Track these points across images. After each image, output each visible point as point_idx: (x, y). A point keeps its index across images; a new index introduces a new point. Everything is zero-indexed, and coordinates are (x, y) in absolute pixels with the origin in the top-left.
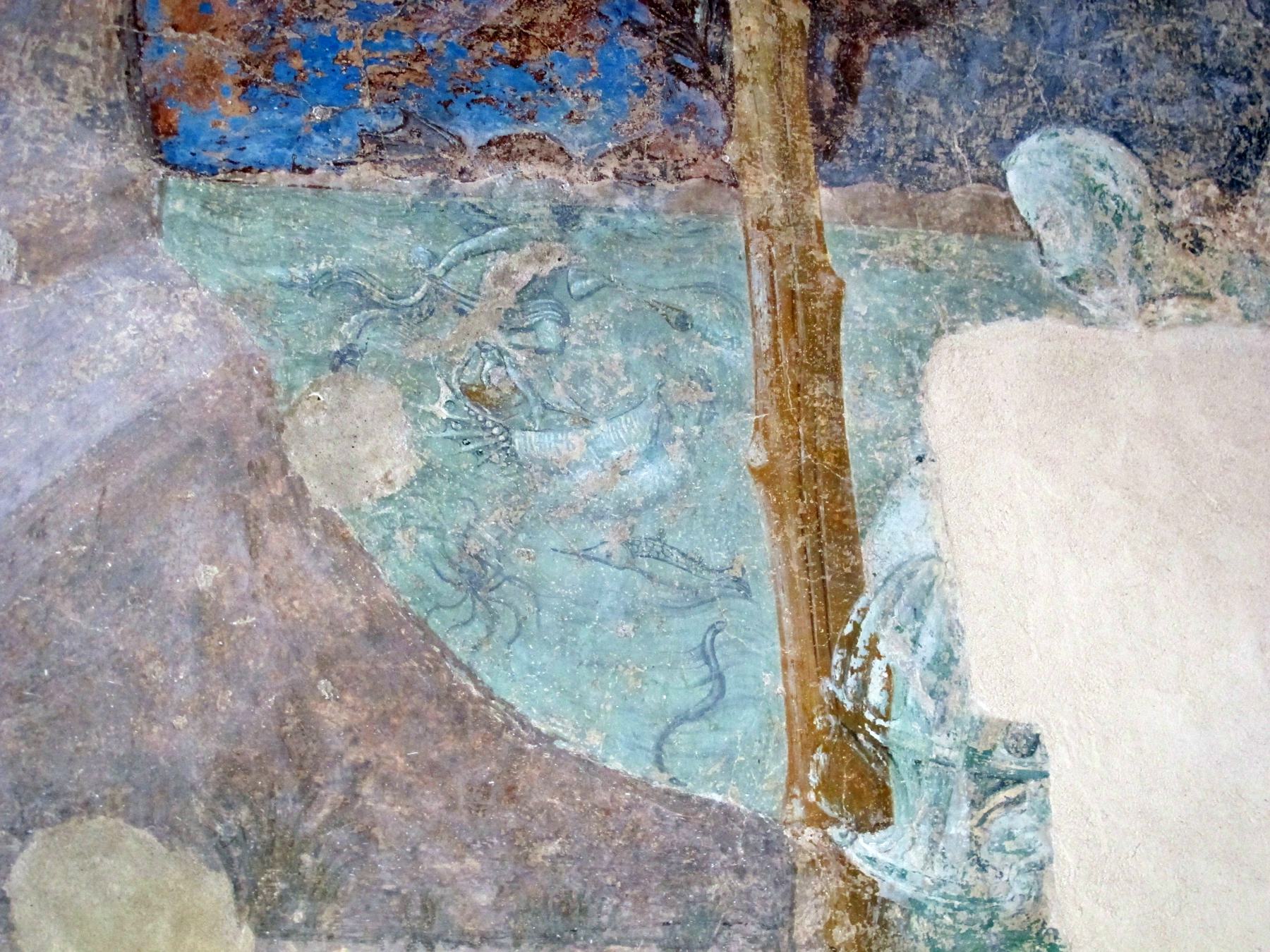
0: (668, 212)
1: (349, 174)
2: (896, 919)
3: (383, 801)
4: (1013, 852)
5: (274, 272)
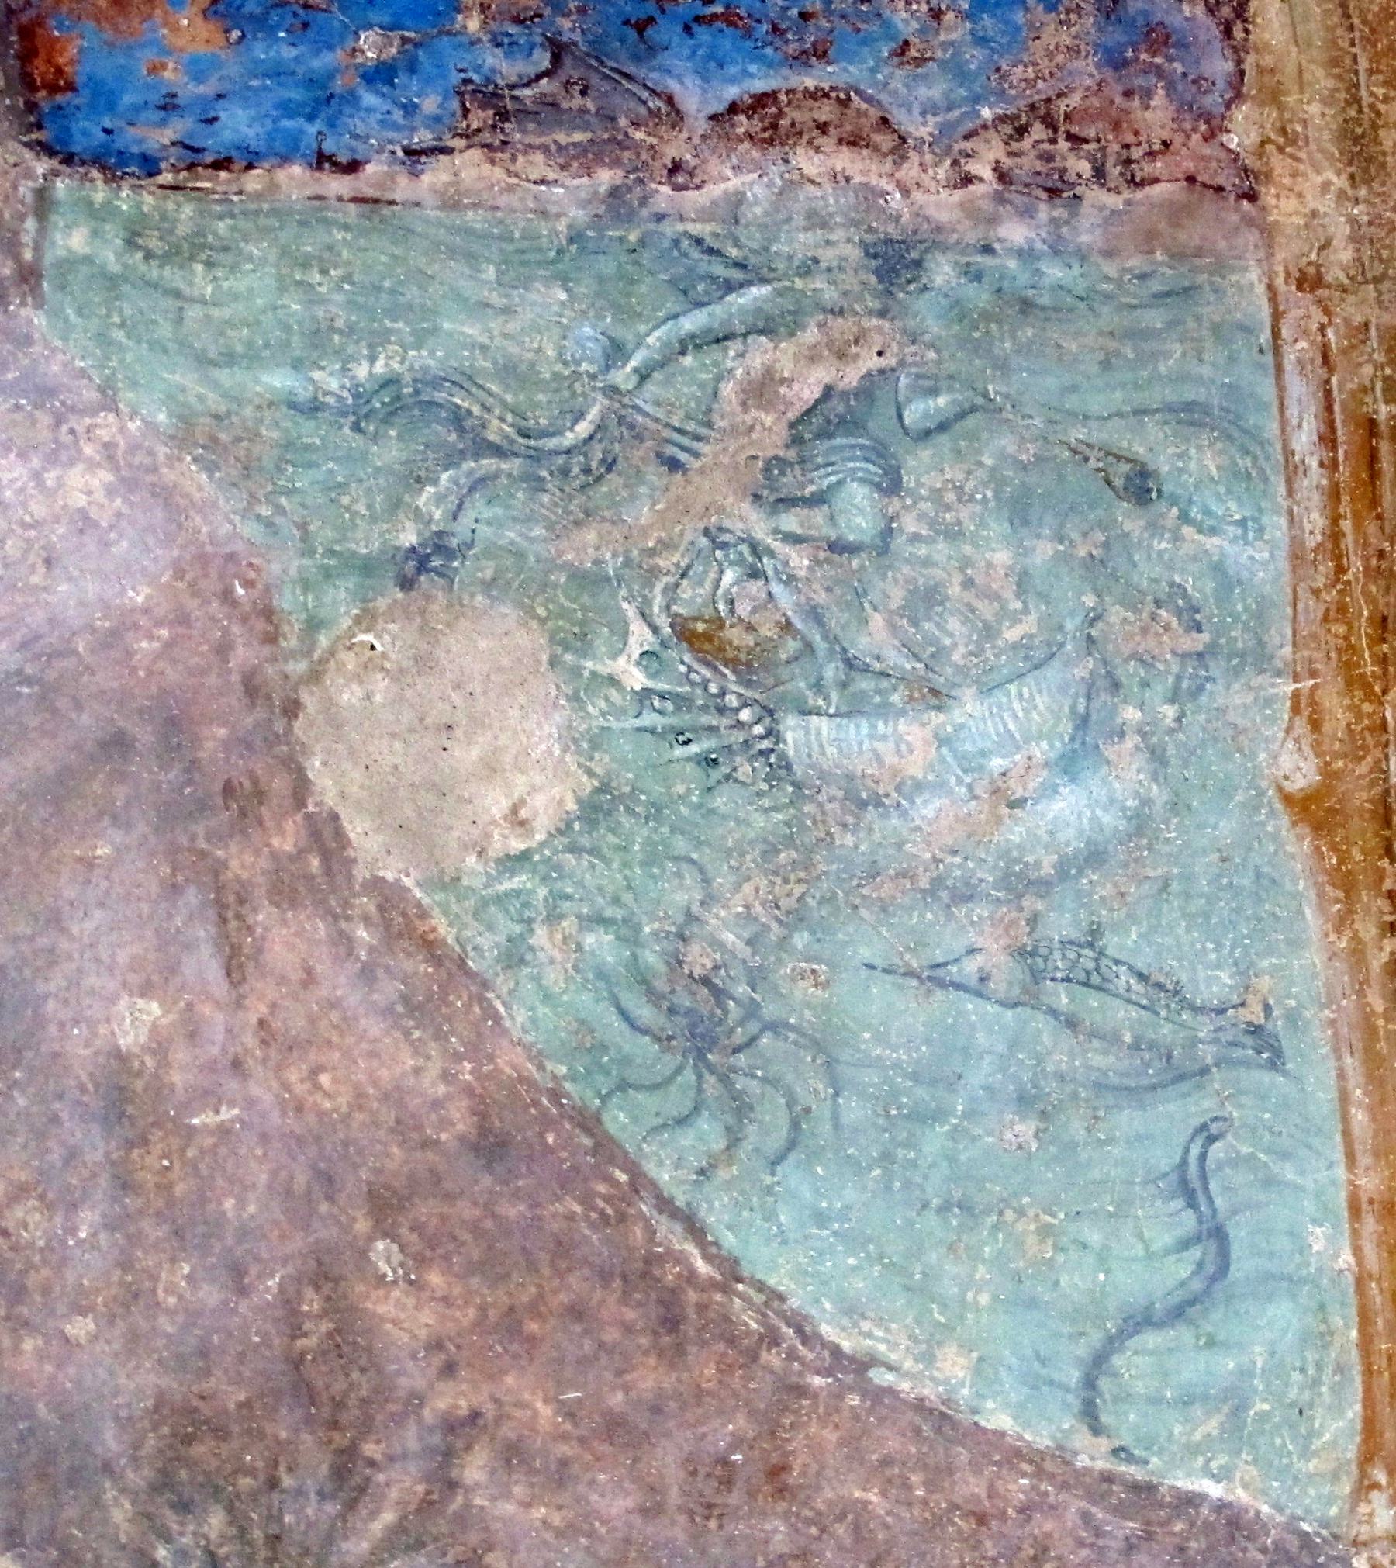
0: (1109, 254)
1: (436, 174)
3: (507, 1495)
5: (279, 380)
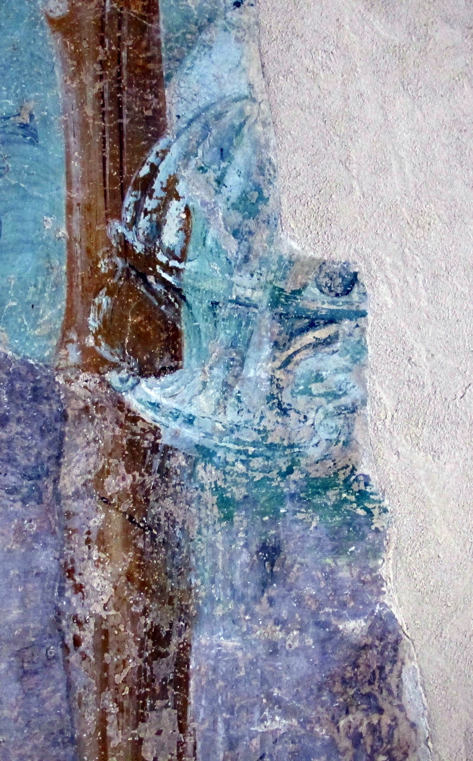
2: (180, 466)
4: (320, 395)
